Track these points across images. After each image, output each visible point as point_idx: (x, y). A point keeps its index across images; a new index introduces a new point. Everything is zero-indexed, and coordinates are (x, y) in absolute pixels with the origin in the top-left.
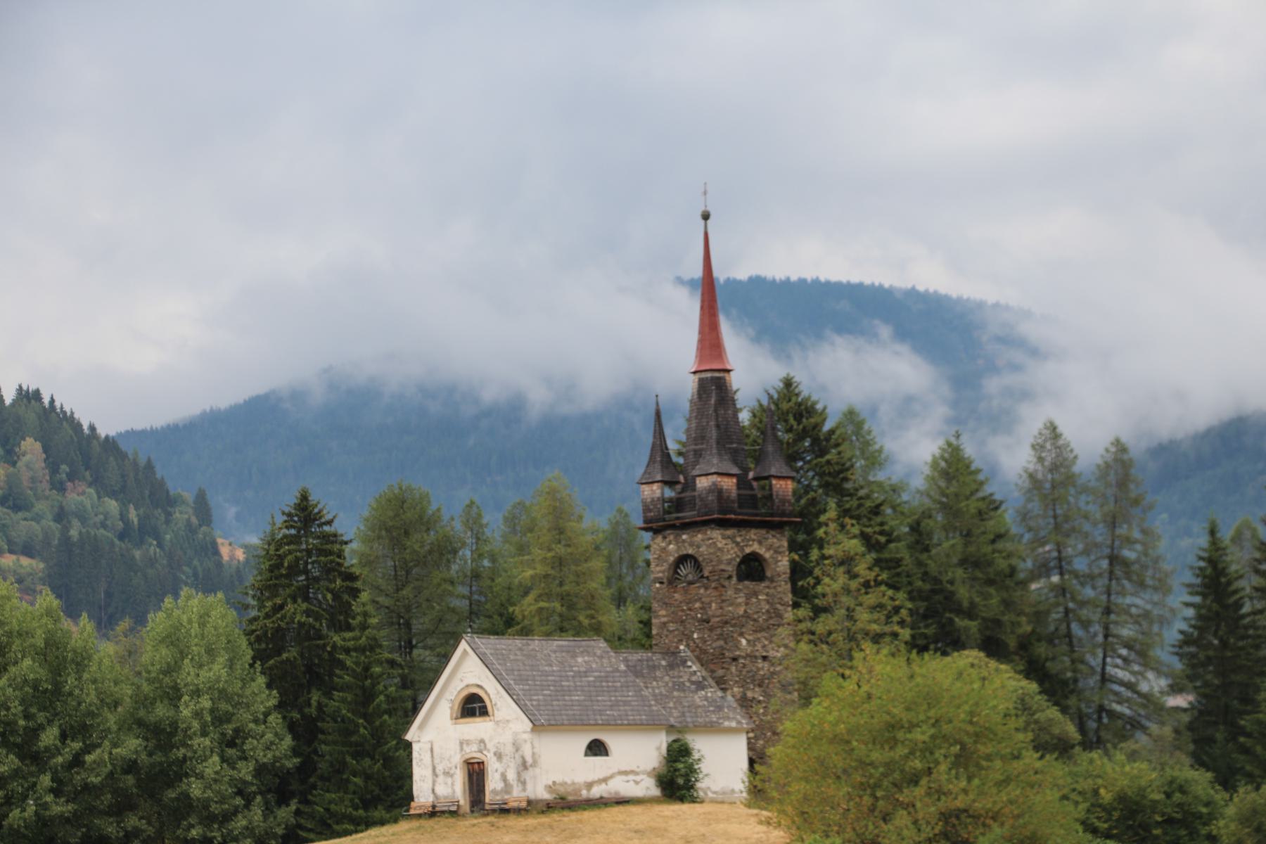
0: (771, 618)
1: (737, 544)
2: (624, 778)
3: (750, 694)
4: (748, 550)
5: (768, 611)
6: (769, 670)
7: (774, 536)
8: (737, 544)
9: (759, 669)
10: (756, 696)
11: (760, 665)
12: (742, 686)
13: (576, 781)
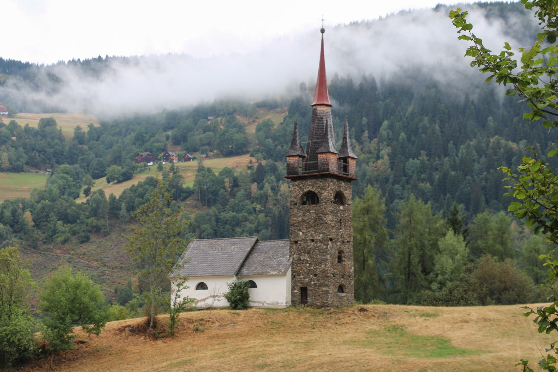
0: (317, 221)
1: (301, 188)
3: (302, 258)
4: (306, 190)
5: (315, 218)
8: (301, 188)
9: (308, 246)
11: (309, 244)
12: (299, 254)
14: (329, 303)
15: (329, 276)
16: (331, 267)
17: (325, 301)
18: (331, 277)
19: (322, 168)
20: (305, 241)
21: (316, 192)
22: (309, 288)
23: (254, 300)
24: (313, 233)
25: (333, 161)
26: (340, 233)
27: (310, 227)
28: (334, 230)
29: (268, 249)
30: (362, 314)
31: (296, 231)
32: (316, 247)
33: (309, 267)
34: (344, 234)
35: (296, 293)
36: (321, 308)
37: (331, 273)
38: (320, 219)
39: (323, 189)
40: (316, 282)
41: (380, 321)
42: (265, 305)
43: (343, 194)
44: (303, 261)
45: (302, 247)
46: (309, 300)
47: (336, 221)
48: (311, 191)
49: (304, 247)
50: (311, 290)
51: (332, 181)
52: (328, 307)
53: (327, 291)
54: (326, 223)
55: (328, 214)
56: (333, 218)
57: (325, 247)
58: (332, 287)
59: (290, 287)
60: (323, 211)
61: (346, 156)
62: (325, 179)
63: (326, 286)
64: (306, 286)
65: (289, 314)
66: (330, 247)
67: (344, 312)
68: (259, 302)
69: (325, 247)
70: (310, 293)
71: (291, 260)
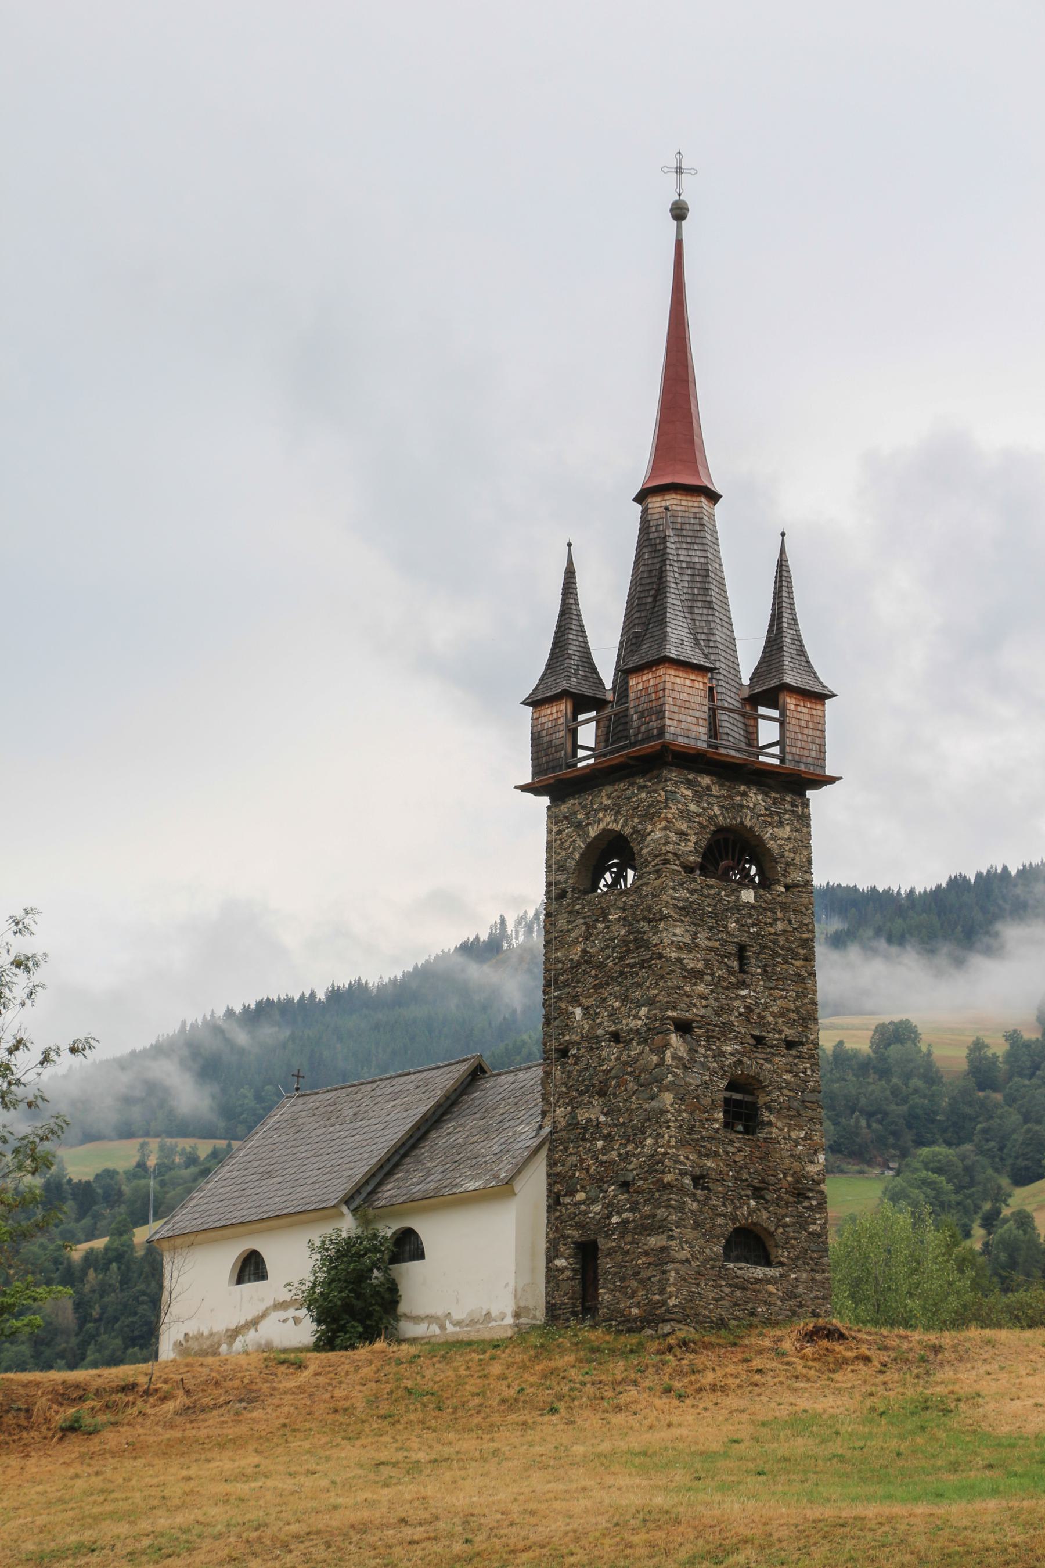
0: (629, 951)
2: (282, 1315)
4: (593, 832)
5: (625, 942)
6: (618, 1059)
7: (641, 788)
8: (579, 825)
10: (593, 1117)
11: (604, 1054)
13: (215, 1330)
14: (672, 1302)
15: (669, 1185)
16: (682, 1143)
17: (657, 1297)
18: (682, 1190)
19: (643, 729)
20: (592, 1041)
21: (627, 831)
22: (604, 1244)
23: (415, 1313)
24: (617, 1004)
25: (684, 696)
26: (737, 1003)
27: (607, 984)
28: (701, 988)
29: (500, 1096)
30: (809, 1350)
31: (563, 1005)
32: (627, 1063)
33: (604, 1151)
34: (766, 1007)
35: (562, 1270)
36: (643, 1328)
37: (682, 1173)
38: (642, 943)
39: (649, 816)
40: (625, 1215)
41: (881, 1378)
42: (450, 1328)
43: (759, 839)
44: (586, 1129)
45: (580, 1071)
46: (605, 1295)
47: (711, 949)
48: (612, 831)
49: (586, 1069)
50: (610, 1253)
51: (690, 783)
52: (664, 1321)
53: (663, 1249)
54: (660, 956)
55: (664, 918)
56: (695, 935)
57: (655, 1059)
58: (690, 1234)
59: (542, 1245)
60: (649, 909)
61: (773, 683)
62: (655, 772)
63: (660, 1227)
64: (592, 1237)
65: (493, 1358)
66: (675, 1057)
67: (735, 1344)
68: (430, 1319)
69: (655, 1059)
70: (606, 1264)
71: (547, 1129)
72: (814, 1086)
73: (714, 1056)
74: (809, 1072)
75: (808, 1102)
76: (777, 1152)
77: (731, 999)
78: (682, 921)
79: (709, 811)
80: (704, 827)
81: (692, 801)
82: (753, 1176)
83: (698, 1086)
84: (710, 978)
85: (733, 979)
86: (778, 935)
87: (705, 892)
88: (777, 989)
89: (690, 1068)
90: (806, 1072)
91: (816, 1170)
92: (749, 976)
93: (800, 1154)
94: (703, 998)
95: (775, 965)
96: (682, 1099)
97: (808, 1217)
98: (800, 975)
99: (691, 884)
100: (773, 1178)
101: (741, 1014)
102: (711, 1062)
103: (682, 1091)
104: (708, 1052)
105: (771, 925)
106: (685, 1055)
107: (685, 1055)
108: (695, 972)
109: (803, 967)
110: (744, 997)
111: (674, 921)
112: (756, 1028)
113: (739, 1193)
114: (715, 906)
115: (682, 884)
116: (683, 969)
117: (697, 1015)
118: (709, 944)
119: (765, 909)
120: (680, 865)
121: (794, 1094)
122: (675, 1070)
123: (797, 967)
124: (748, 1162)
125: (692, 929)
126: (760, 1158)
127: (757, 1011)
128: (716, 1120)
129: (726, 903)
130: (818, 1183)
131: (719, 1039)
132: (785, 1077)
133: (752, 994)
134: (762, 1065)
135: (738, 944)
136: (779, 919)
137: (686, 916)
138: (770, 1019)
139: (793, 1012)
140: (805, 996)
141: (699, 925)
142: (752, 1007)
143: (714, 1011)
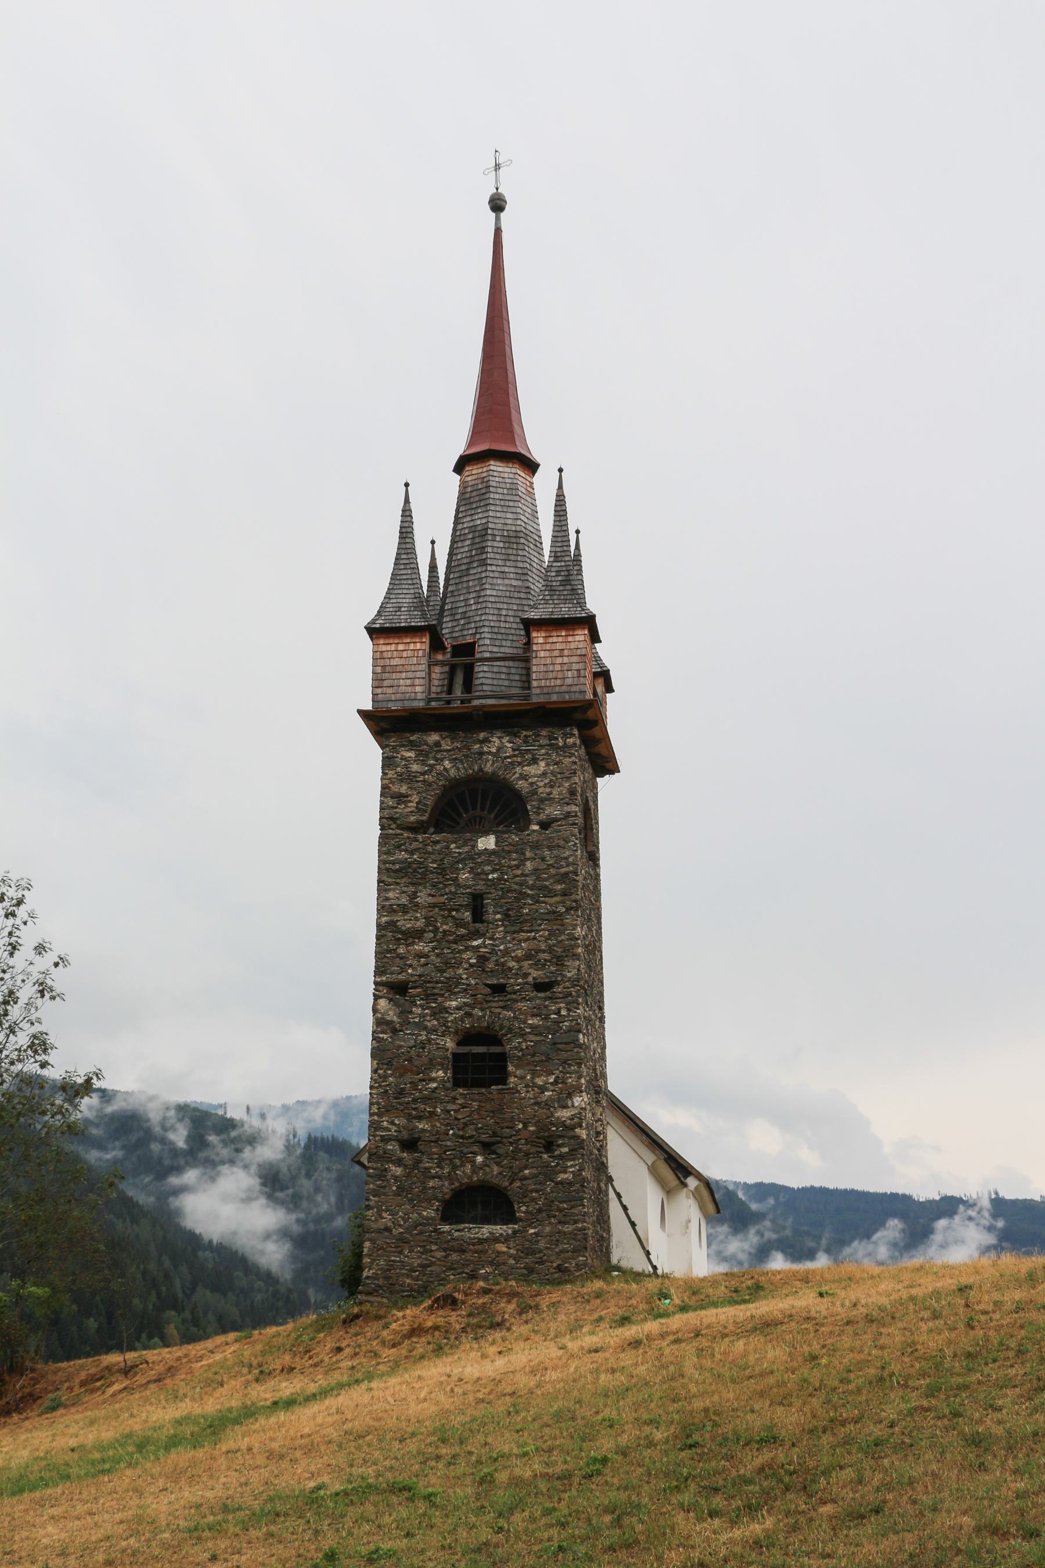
28: (420, 947)
34: (506, 952)
47: (434, 905)
56: (415, 895)
72: (570, 1026)
73: (433, 1015)
74: (564, 1012)
75: (560, 1043)
76: (516, 1102)
77: (460, 952)
78: (397, 884)
79: (438, 767)
80: (430, 785)
81: (415, 761)
82: (481, 1131)
83: (411, 1048)
84: (431, 935)
85: (463, 931)
86: (526, 875)
87: (430, 848)
88: (523, 931)
89: (401, 1031)
90: (559, 1012)
91: (569, 1114)
92: (485, 924)
93: (547, 1100)
94: (422, 957)
95: (522, 908)
96: (389, 1064)
97: (556, 1166)
98: (554, 912)
99: (410, 845)
100: (508, 1130)
101: (472, 965)
102: (429, 1021)
103: (389, 1054)
104: (426, 1011)
105: (517, 867)
106: (395, 1018)
107: (395, 1018)
108: (409, 933)
109: (558, 903)
110: (478, 947)
111: (387, 885)
112: (493, 976)
113: (461, 1152)
114: (442, 860)
115: (398, 847)
116: (395, 932)
117: (412, 975)
118: (430, 900)
119: (510, 852)
120: (397, 828)
121: (543, 1038)
122: (381, 1036)
123: (551, 905)
124: (477, 1117)
125: (412, 889)
126: (493, 1112)
127: (494, 959)
128: (434, 1080)
129: (456, 855)
130: (572, 1128)
131: (442, 995)
132: (530, 1022)
133: (488, 942)
134: (499, 1014)
135: (470, 894)
136: (528, 859)
137: (403, 877)
138: (512, 964)
139: (544, 951)
140: (562, 933)
141: (420, 884)
142: (487, 955)
143: (436, 967)
